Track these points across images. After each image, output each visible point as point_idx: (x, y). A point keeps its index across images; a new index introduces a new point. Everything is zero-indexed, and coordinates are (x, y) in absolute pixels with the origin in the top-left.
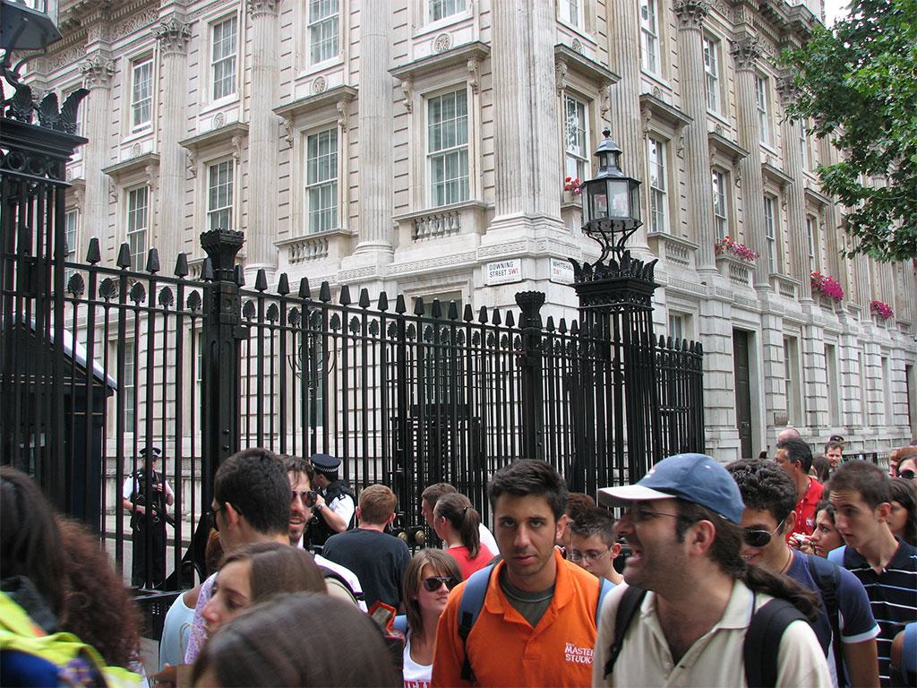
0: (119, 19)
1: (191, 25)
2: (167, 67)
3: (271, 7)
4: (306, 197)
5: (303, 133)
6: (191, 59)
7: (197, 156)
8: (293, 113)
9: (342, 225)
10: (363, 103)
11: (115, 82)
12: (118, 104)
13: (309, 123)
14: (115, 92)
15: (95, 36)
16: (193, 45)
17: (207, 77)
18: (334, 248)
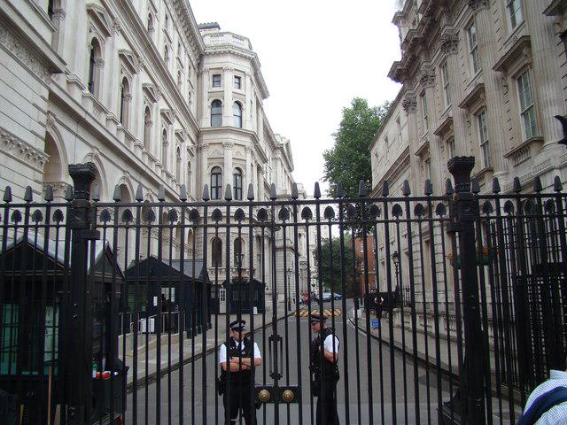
0: (432, 45)
1: (457, 34)
2: (453, 60)
3: (484, 4)
4: (522, 120)
5: (514, 77)
6: (460, 53)
7: (469, 112)
8: (503, 66)
9: (539, 134)
10: (538, 44)
11: (436, 81)
12: (438, 94)
13: (514, 69)
14: (438, 87)
15: (423, 58)
16: (460, 46)
17: (469, 61)
18: (533, 149)
